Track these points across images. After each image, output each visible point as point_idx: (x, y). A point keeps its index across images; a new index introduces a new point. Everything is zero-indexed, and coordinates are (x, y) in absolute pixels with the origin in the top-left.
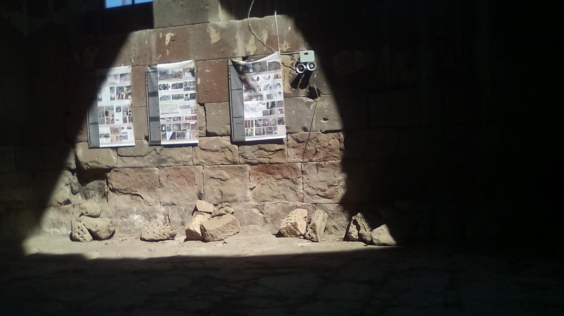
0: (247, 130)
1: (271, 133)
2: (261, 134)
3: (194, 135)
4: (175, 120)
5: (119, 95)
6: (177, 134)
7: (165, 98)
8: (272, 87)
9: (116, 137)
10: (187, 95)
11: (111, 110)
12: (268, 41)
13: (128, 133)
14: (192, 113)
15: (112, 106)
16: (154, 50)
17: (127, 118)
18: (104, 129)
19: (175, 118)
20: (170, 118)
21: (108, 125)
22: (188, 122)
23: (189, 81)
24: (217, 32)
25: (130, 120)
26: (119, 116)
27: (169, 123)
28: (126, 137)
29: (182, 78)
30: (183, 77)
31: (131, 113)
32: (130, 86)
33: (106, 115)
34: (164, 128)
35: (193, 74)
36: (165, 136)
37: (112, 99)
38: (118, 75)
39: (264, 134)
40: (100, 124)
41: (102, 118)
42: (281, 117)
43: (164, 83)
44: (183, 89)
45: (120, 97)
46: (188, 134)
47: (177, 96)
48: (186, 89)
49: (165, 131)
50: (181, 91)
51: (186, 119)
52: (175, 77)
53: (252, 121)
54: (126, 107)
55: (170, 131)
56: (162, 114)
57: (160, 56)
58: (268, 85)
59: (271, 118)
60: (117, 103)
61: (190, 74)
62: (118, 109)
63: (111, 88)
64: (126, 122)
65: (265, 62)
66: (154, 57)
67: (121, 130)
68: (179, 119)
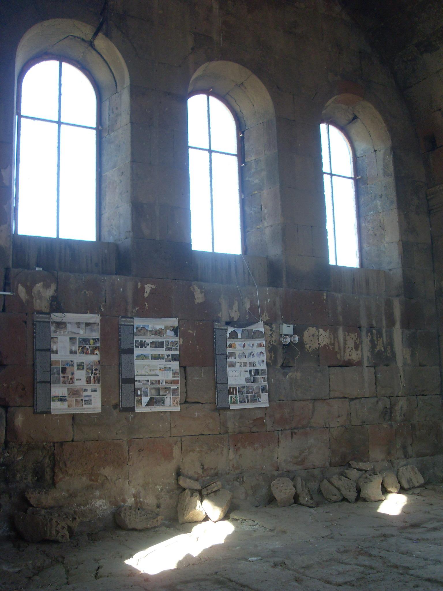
0: (231, 397)
1: (255, 401)
2: (245, 402)
3: (174, 401)
4: (153, 383)
5: (82, 349)
6: (155, 399)
7: (144, 357)
8: (255, 355)
9: (76, 401)
10: (168, 356)
11: (69, 366)
13: (92, 396)
14: (173, 377)
15: (72, 361)
16: (130, 300)
17: (92, 378)
18: (58, 390)
19: (153, 380)
20: (148, 381)
21: (65, 385)
22: (168, 386)
23: (170, 340)
24: (202, 292)
25: (95, 381)
26: (81, 375)
27: (145, 386)
28: (89, 402)
29: (164, 336)
30: (165, 335)
31: (97, 372)
32: (98, 339)
33: (62, 372)
34: (139, 391)
35: (176, 334)
36: (140, 402)
37: (72, 352)
38: (82, 323)
39: (248, 402)
40: (53, 384)
41: (56, 376)
42: (264, 385)
43: (141, 340)
44: (164, 349)
45: (83, 351)
46: (168, 400)
47: (157, 356)
48: (167, 349)
50: (161, 351)
53: (236, 388)
54: (91, 364)
55: (147, 396)
56: (137, 375)
57: (137, 308)
58: (252, 352)
59: (254, 386)
60: (79, 358)
61: (172, 333)
62: (81, 366)
63: (71, 339)
64: (90, 383)
66: (130, 308)
67: (83, 393)
68: (158, 382)
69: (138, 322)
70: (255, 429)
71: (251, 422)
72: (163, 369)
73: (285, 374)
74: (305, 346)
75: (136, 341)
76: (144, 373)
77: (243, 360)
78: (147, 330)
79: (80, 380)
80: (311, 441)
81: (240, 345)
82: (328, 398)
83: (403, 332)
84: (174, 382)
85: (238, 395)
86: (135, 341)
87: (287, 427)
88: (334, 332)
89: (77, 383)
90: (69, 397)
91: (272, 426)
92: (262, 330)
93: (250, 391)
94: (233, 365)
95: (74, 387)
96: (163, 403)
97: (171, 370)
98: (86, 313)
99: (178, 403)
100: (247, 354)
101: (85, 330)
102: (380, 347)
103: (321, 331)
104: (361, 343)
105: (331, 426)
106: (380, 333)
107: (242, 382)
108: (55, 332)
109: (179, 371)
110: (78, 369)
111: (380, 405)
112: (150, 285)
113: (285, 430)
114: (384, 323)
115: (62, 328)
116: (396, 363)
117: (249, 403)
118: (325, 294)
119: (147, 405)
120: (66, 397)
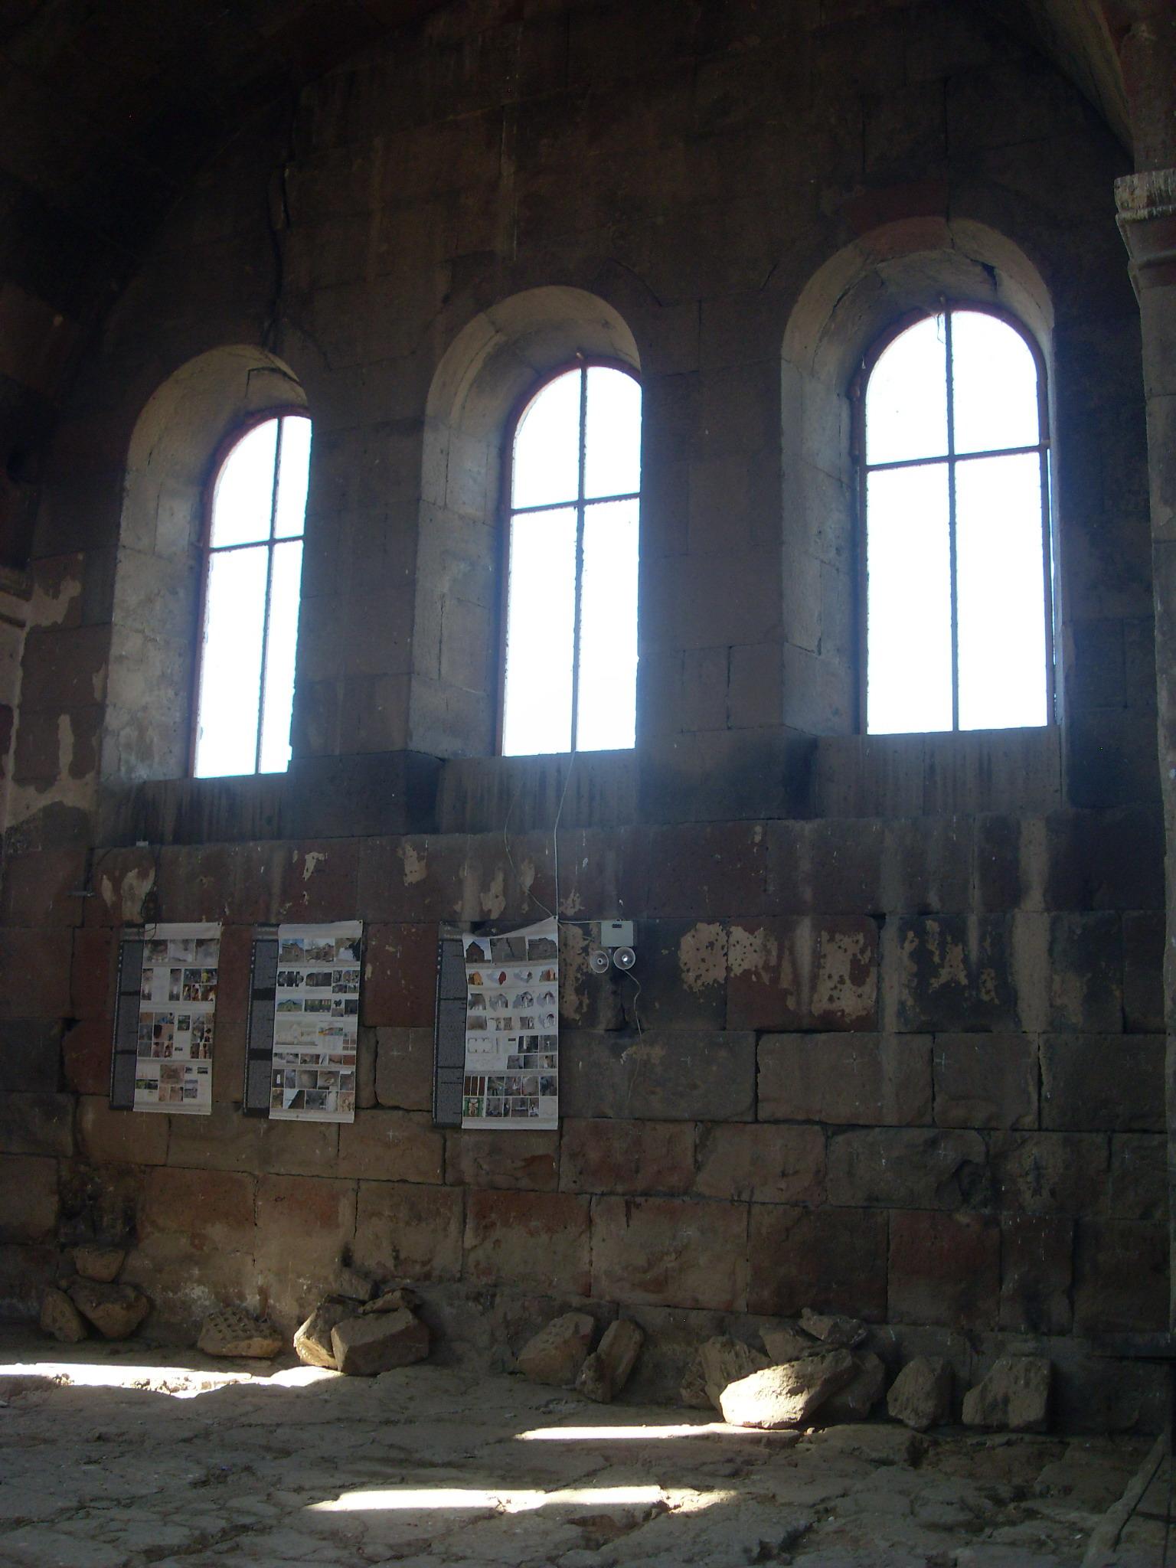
1: (523, 1113)
2: (499, 1115)
3: (344, 1102)
4: (304, 1061)
6: (308, 1096)
7: (291, 1006)
8: (535, 1000)
9: (173, 1089)
10: (338, 1003)
12: (532, 888)
14: (345, 1048)
15: (171, 1014)
16: (276, 890)
17: (201, 1048)
18: (147, 1068)
19: (306, 1055)
20: (297, 1055)
21: (157, 1058)
22: (334, 1067)
23: (344, 969)
24: (420, 858)
25: (206, 1053)
26: (183, 1040)
27: (291, 1067)
28: (193, 1093)
29: (333, 960)
30: (335, 959)
31: (211, 1035)
34: (279, 1076)
35: (357, 956)
36: (279, 1098)
37: (173, 997)
38: (192, 940)
39: (506, 1115)
40: (139, 1056)
41: (146, 1040)
42: (549, 1075)
43: (290, 970)
44: (331, 988)
45: (191, 996)
46: (331, 1099)
47: (317, 1002)
48: (337, 989)
49: (281, 1085)
50: (325, 993)
51: (330, 1060)
52: (317, 957)
53: (482, 1079)
54: (201, 1019)
55: (293, 1087)
56: (277, 1044)
57: (288, 905)
58: (525, 993)
59: (525, 1076)
62: (184, 1023)
65: (522, 939)
66: (275, 906)
69: (286, 933)
70: (524, 1183)
71: (521, 1164)
72: (327, 1032)
73: (617, 1051)
74: (683, 975)
75: (280, 972)
76: (289, 1039)
77: (503, 1013)
78: (301, 949)
79: (182, 1050)
80: (690, 1232)
81: (490, 977)
82: (750, 1119)
83: (1054, 924)
84: (346, 1060)
85: (485, 1097)
87: (620, 1189)
88: (783, 934)
89: (176, 1056)
90: (162, 1082)
91: (574, 1179)
92: (554, 937)
93: (515, 1087)
94: (480, 1025)
95: (171, 1064)
96: (322, 1104)
97: (341, 1035)
98: (200, 921)
99: (351, 1107)
100: (511, 998)
101: (197, 952)
102: (952, 970)
103: (738, 933)
104: (877, 961)
105: (757, 1197)
106: (954, 930)
107: (500, 1066)
108: (150, 959)
110: (180, 1028)
111: (947, 1154)
112: (315, 854)
113: (612, 1193)
114: (975, 895)
115: (161, 952)
116: (1018, 1022)
117: (509, 1118)
118: (758, 829)
119: (291, 1107)
120: (157, 1080)
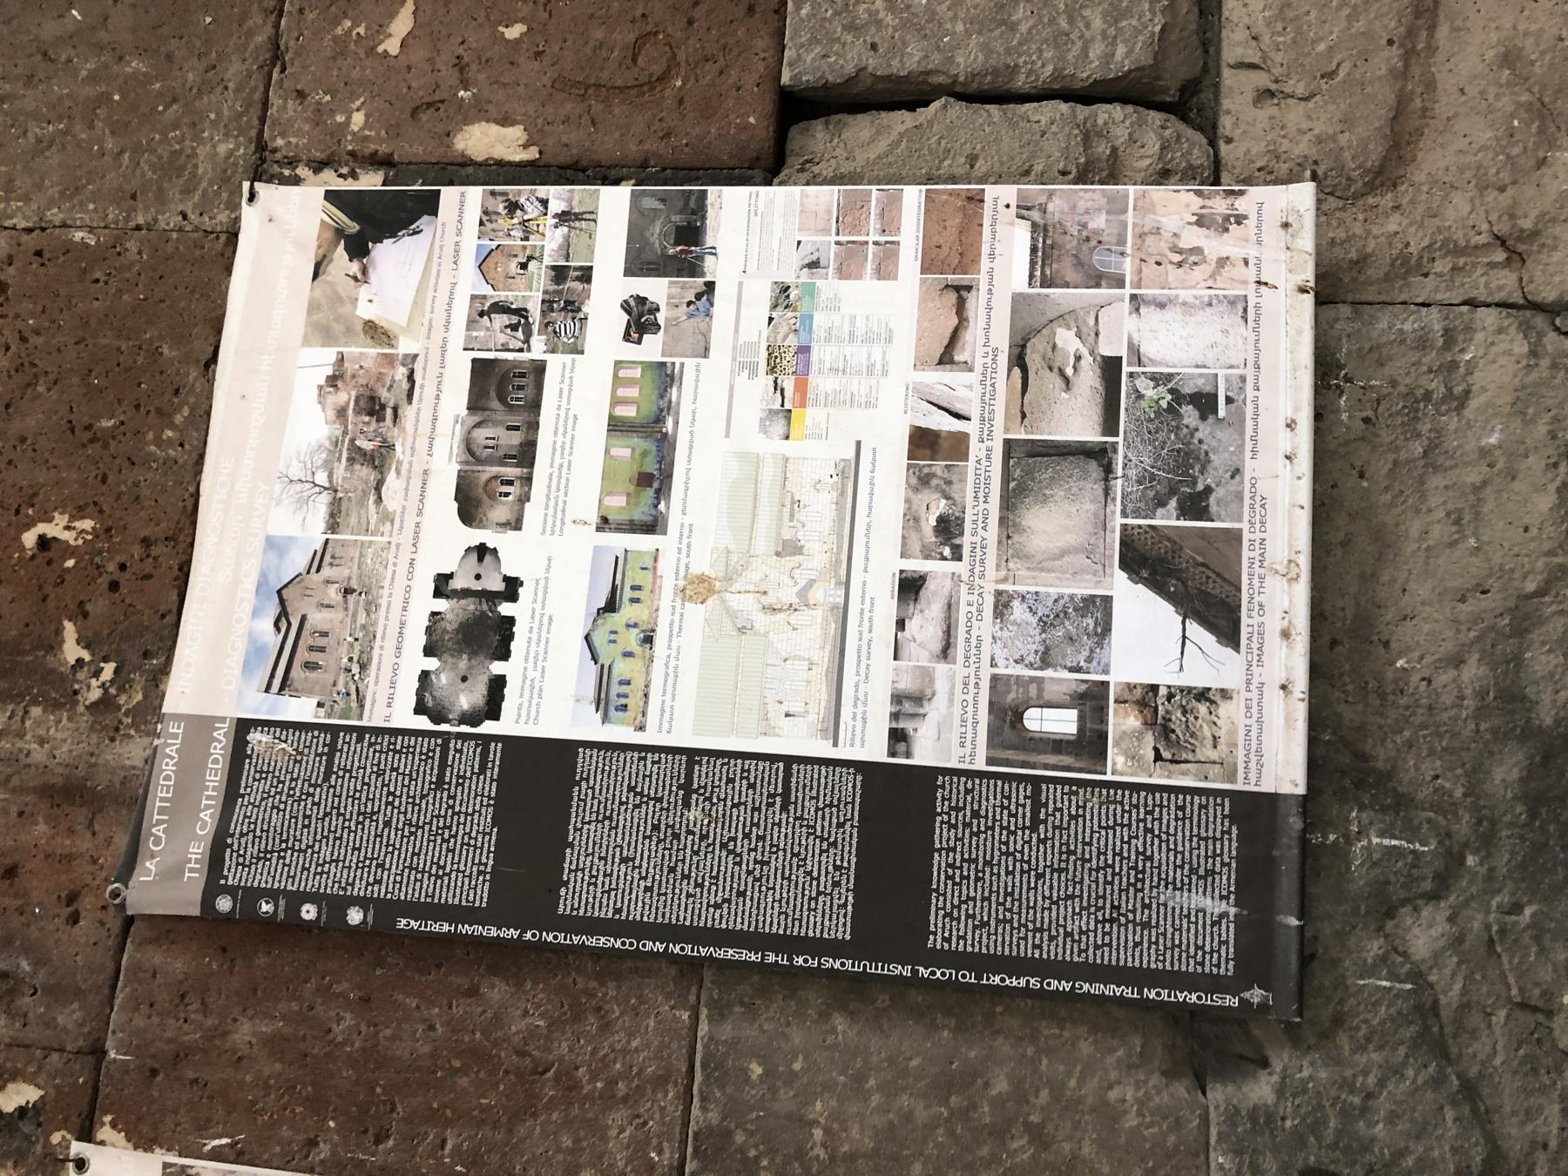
3: (1189, 257)
4: (948, 528)
10: (640, 320)
19: (912, 519)
20: (910, 587)
23: (469, 282)
30: (405, 346)
34: (1040, 721)
47: (623, 452)
49: (1092, 701)
51: (946, 359)
52: (378, 460)
55: (1100, 608)
57: (72, 651)
68: (938, 466)
72: (788, 384)
75: (420, 709)
86: (423, 723)
96: (1205, 403)
97: (810, 290)
99: (1220, 206)
109: (826, 196)
119: (1229, 633)
